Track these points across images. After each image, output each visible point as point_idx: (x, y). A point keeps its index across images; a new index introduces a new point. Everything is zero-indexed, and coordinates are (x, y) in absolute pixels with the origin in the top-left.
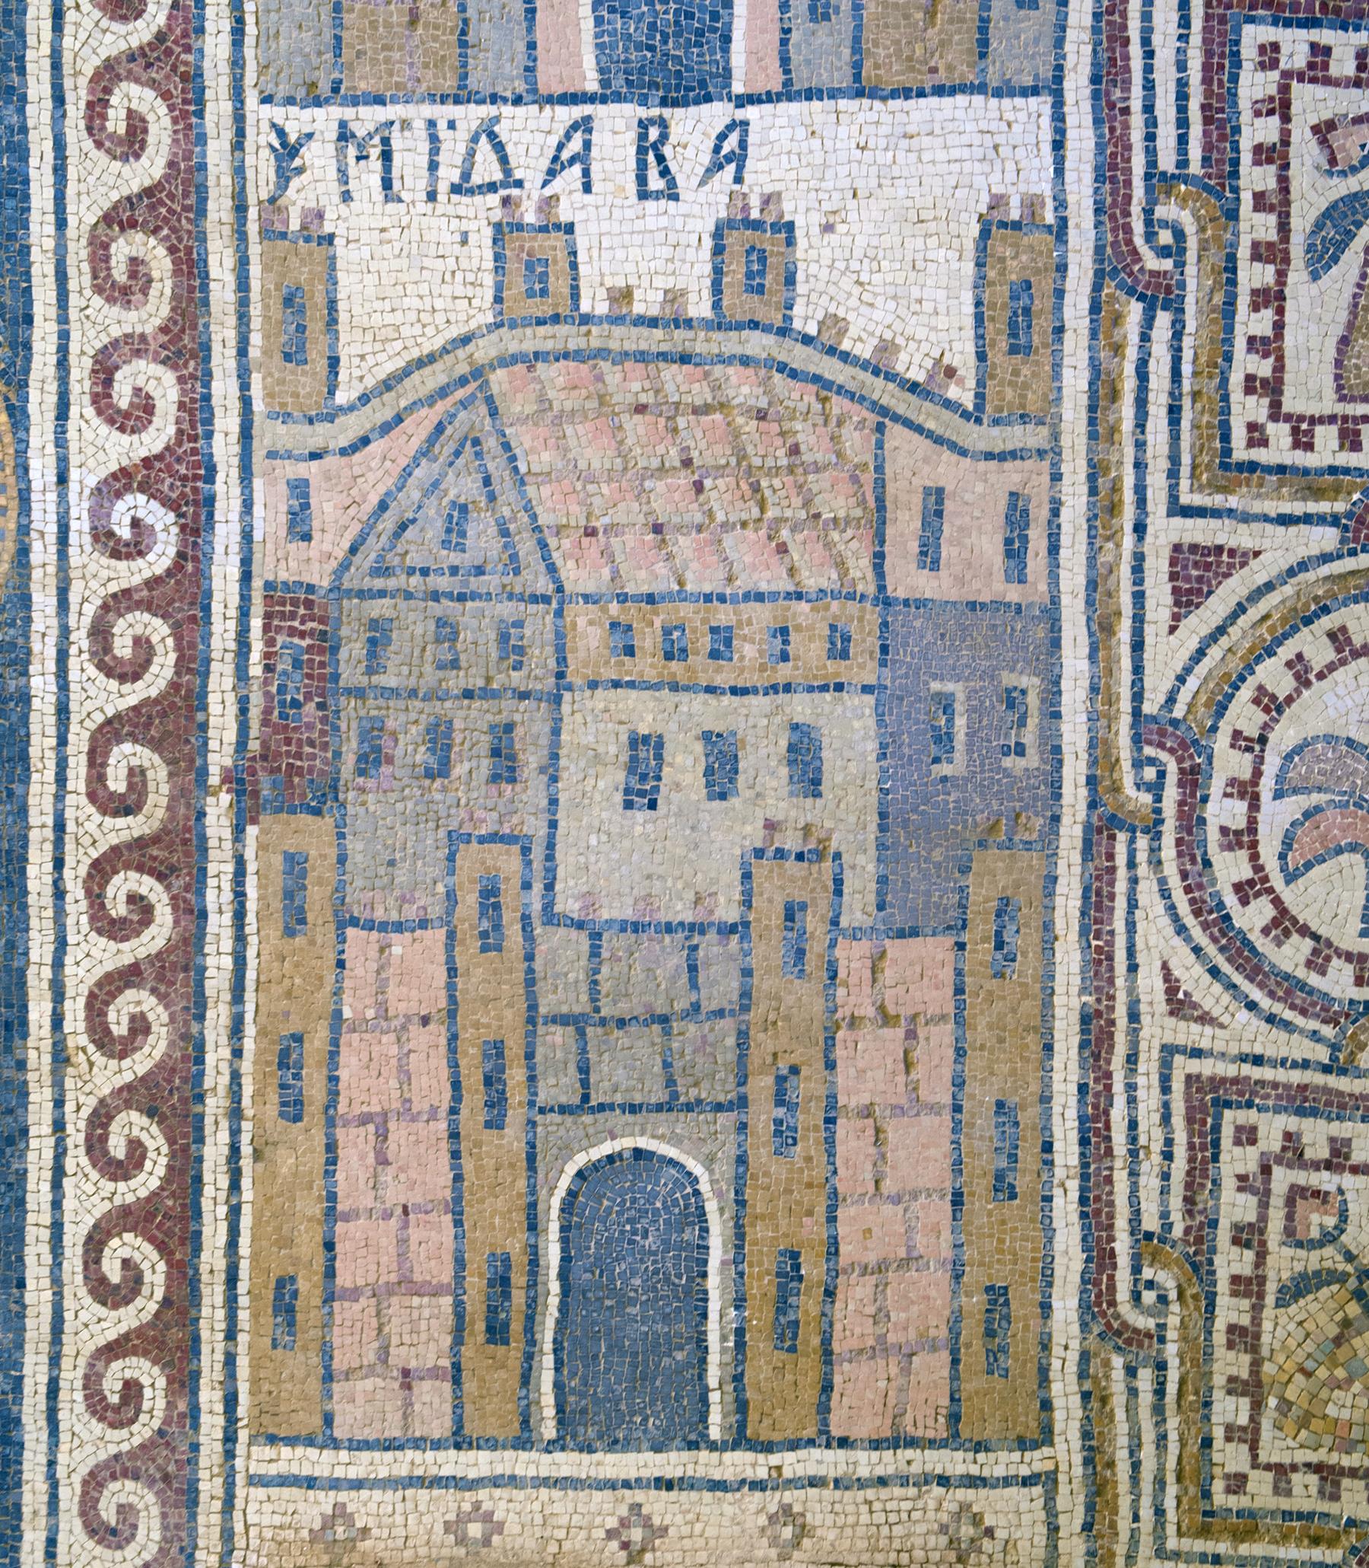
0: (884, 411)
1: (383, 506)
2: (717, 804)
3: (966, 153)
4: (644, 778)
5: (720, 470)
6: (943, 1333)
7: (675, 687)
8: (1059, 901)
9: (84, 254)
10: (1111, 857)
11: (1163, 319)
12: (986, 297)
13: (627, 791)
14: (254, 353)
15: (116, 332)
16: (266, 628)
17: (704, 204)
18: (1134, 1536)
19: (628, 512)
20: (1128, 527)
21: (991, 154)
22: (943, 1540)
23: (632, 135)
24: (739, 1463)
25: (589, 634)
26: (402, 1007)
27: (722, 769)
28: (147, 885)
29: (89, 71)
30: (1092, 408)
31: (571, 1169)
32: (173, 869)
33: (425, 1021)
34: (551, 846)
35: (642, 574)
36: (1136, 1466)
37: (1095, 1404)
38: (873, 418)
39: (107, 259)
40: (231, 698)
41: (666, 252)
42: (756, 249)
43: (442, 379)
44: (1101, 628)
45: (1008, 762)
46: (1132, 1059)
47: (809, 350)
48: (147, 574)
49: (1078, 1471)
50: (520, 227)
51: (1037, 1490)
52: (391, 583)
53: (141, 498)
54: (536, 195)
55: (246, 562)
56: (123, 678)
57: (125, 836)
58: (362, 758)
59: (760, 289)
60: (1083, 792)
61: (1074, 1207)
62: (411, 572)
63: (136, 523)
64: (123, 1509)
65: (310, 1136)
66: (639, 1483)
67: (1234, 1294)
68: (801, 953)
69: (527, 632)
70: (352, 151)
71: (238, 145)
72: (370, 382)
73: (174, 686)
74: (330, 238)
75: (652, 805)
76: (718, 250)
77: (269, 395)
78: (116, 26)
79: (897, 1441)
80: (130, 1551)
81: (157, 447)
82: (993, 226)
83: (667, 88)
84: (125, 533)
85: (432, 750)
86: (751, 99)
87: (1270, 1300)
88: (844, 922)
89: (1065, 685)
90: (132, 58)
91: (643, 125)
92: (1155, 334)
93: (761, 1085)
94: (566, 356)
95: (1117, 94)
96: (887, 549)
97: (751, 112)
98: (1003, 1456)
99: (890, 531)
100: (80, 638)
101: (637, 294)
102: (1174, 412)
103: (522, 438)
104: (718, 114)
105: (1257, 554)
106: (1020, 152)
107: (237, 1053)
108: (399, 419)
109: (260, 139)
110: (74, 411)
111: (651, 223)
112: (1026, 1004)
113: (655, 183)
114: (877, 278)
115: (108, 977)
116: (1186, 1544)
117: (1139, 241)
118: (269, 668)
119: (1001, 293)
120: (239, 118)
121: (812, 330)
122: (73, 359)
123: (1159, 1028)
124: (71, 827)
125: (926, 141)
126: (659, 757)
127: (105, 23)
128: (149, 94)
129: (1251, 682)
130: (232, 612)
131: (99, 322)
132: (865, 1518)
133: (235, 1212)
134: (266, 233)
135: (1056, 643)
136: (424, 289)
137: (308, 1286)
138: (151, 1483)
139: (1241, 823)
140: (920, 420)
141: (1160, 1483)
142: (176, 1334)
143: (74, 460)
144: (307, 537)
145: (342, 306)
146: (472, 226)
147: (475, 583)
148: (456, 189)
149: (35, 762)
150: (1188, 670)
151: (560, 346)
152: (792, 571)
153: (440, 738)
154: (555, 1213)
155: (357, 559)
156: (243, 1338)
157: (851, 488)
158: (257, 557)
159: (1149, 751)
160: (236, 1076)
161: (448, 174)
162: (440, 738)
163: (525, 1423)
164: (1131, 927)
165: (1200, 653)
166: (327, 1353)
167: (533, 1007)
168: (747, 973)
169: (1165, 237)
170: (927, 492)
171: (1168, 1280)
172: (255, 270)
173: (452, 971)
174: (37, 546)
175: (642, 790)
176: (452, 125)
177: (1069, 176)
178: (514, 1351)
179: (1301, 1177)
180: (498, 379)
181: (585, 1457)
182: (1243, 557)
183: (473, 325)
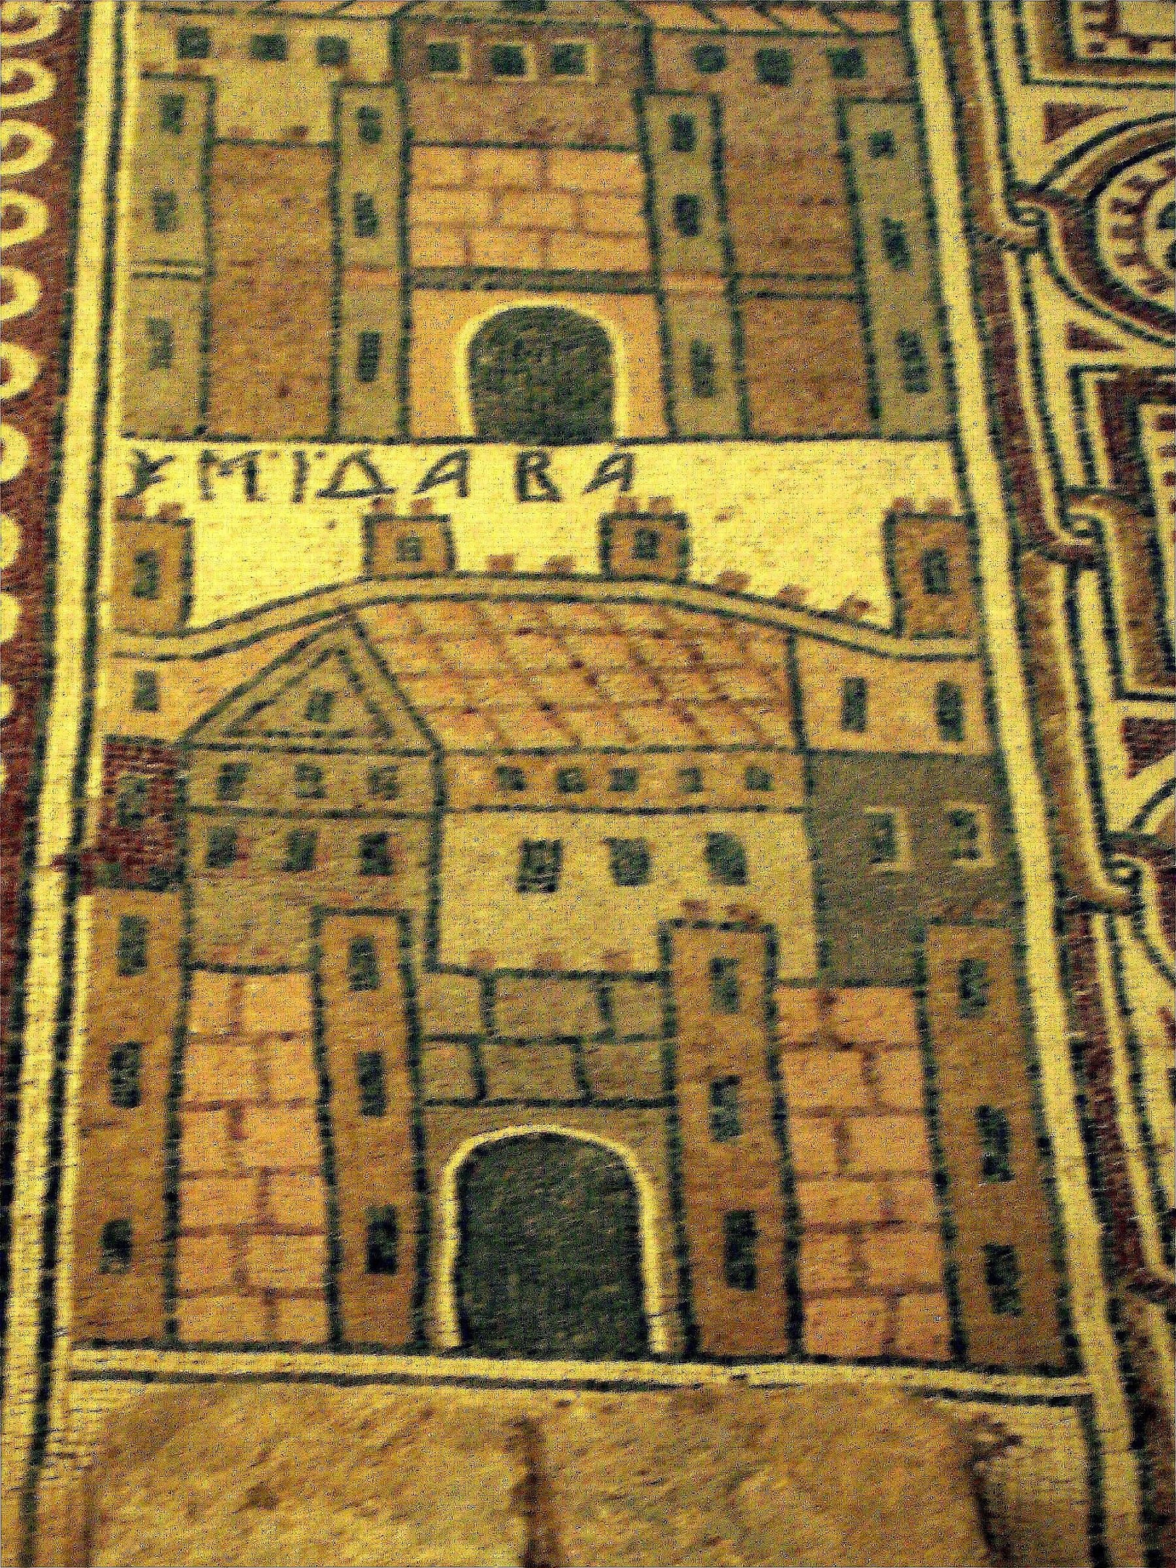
4: (540, 870)
16: (107, 765)
33: (287, 1037)
34: (433, 918)
45: (962, 863)
46: (1136, 1078)
50: (390, 517)
93: (694, 1093)
95: (1017, 442)
102: (1110, 634)
107: (62, 1056)
113: (535, 489)
134: (121, 516)
148: (323, 494)
159: (1118, 857)
169: (1082, 526)
178: (404, 1279)
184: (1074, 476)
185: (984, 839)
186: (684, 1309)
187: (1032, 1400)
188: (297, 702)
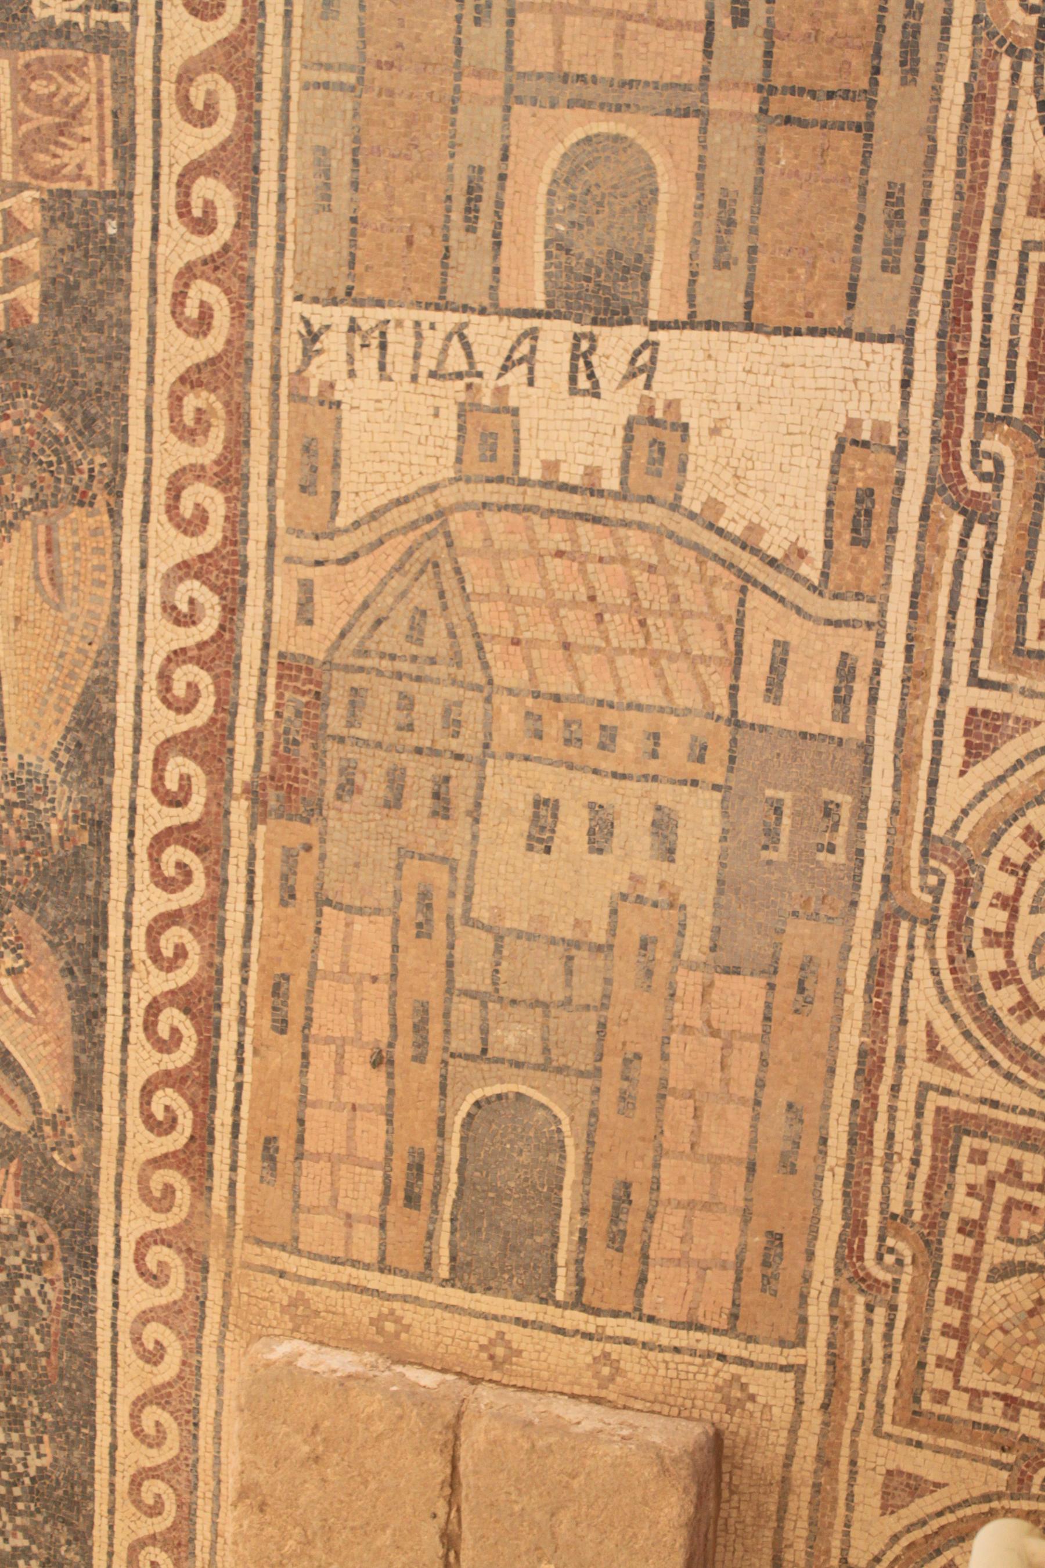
0: (747, 578)
1: (365, 605)
2: (595, 857)
3: (830, 383)
4: (543, 829)
5: (618, 609)
6: (732, 1258)
7: (571, 767)
8: (851, 965)
9: (165, 404)
10: (895, 938)
11: (979, 531)
12: (837, 497)
13: (530, 837)
14: (279, 484)
15: (185, 462)
16: (278, 685)
17: (620, 402)
18: (859, 1419)
19: (547, 631)
20: (934, 690)
21: (851, 386)
22: (718, 1396)
23: (567, 346)
24: (574, 1319)
25: (510, 720)
26: (359, 968)
27: (601, 833)
28: (189, 857)
29: (175, 271)
30: (914, 595)
31: (471, 1099)
32: (207, 848)
33: (375, 979)
34: (471, 868)
35: (552, 679)
36: (866, 1372)
37: (839, 1325)
38: (740, 582)
39: (181, 407)
40: (252, 733)
41: (589, 437)
42: (658, 438)
43: (414, 516)
44: (904, 767)
45: (821, 856)
47: (693, 524)
48: (198, 638)
49: (822, 1367)
50: (478, 407)
51: (791, 1376)
52: (368, 663)
53: (197, 584)
54: (492, 384)
55: (266, 636)
56: (178, 710)
57: (176, 822)
58: (341, 787)
59: (659, 474)
60: (878, 887)
61: (839, 1187)
62: (382, 656)
63: (192, 601)
64: (160, 1264)
65: (290, 1045)
66: (503, 1319)
67: (955, 1267)
68: (649, 973)
69: (465, 709)
70: (358, 341)
71: (277, 329)
72: (362, 513)
73: (213, 720)
74: (339, 404)
75: (548, 850)
76: (628, 439)
77: (289, 516)
78: (195, 238)
79: (692, 1325)
80: (165, 1290)
81: (209, 548)
82: (849, 443)
83: (597, 311)
84: (184, 608)
85: (390, 788)
86: (664, 326)
87: (983, 1275)
88: (684, 956)
89: (871, 804)
90: (205, 262)
91: (577, 337)
92: (971, 542)
93: (612, 1063)
94: (506, 507)
95: (958, 347)
96: (741, 684)
97: (661, 336)
98: (767, 1348)
99: (744, 669)
100: (151, 681)
101: (563, 467)
102: (981, 605)
103: (469, 565)
104: (635, 334)
105: (1037, 723)
106: (875, 388)
107: (245, 981)
108: (381, 542)
109: (291, 328)
110: (153, 517)
111: (578, 414)
112: (817, 1038)
113: (583, 383)
114: (750, 474)
115: (162, 916)
116: (896, 1430)
117: (965, 467)
118: (278, 715)
119: (847, 498)
120: (278, 309)
121: (696, 508)
122: (154, 479)
123: (919, 1069)
124: (140, 810)
125: (798, 371)
126: (555, 816)
127: (188, 236)
128: (216, 290)
129: (1022, 822)
130: (256, 672)
131: (173, 454)
132: (662, 1372)
133: (239, 1087)
135: (867, 772)
136: (404, 447)
137: (286, 1147)
138: (179, 1251)
139: (1002, 928)
140: (776, 587)
141: (883, 1387)
142: (196, 1160)
143: (152, 552)
144: (310, 622)
145: (344, 455)
146: (442, 403)
147: (428, 670)
148: (433, 375)
149: (118, 763)
150: (971, 806)
151: (503, 500)
152: (667, 691)
153: (396, 780)
154: (457, 1127)
155: (345, 642)
156: (241, 1173)
157: (717, 634)
158: (274, 634)
159: (933, 863)
160: (243, 996)
161: (428, 363)
162: (396, 780)
163: (428, 1264)
164: (905, 992)
165: (983, 795)
166: (296, 1193)
167: (451, 981)
168: (608, 981)
169: (988, 466)
170: (776, 643)
171: (906, 1251)
172: (284, 424)
173: (395, 948)
174: (124, 612)
175: (541, 838)
176: (432, 327)
177: (913, 410)
179: (1019, 1194)
180: (456, 521)
181: (468, 1295)
182: (1027, 724)
183: (439, 478)
184: (994, 406)
185: (840, 841)
186: (579, 1262)
187: (768, 1366)
188: (401, 619)
